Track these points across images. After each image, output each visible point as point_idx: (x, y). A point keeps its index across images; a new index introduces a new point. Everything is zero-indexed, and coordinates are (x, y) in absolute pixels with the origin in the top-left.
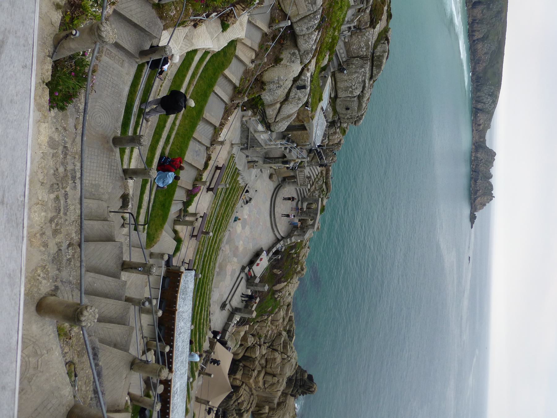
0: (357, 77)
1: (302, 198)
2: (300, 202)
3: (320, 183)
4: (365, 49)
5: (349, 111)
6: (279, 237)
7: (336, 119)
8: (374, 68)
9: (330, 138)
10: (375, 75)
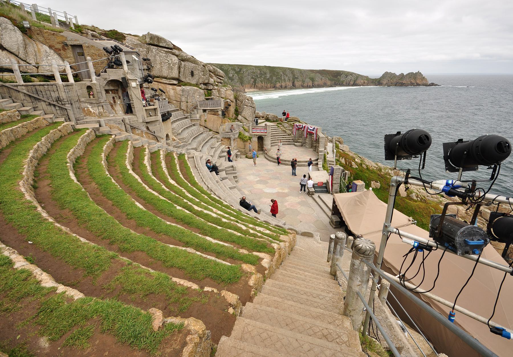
0: (160, 56)
2: (296, 144)
4: (141, 49)
5: (195, 73)
7: (203, 86)
8: (160, 44)
10: (168, 45)
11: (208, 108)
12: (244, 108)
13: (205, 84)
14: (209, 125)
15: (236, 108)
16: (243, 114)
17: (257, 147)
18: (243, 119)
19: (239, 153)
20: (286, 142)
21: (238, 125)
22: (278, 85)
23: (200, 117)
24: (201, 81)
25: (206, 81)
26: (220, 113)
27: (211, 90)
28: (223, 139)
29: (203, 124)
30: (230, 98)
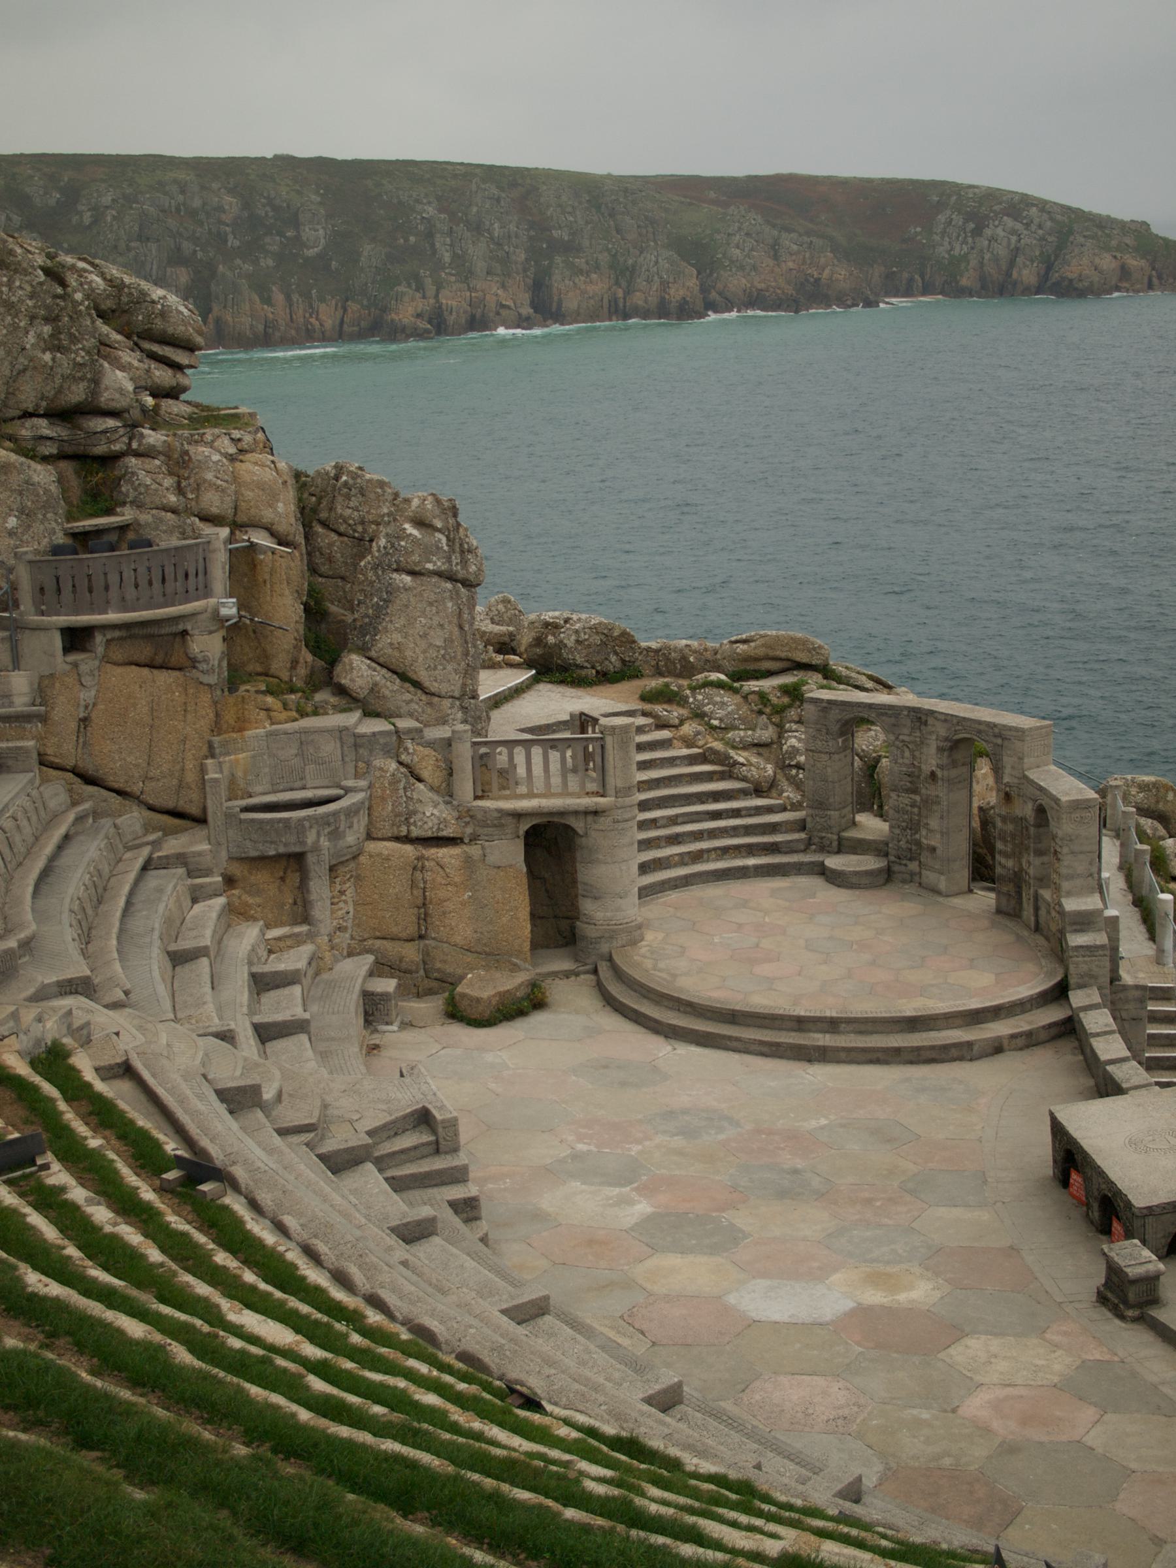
1: (807, 846)
2: (833, 862)
3: (723, 705)
6: (1052, 1015)
9: (213, 502)
11: (112, 617)
12: (391, 591)
13: (64, 415)
14: (118, 757)
15: (312, 592)
16: (385, 641)
17: (524, 913)
18: (390, 686)
19: (388, 985)
20: (750, 850)
21: (358, 743)
22: (408, 309)
23: (42, 691)
24: (29, 394)
25: (77, 394)
26: (208, 646)
27: (111, 459)
28: (237, 870)
29: (67, 750)
30: (268, 515)
